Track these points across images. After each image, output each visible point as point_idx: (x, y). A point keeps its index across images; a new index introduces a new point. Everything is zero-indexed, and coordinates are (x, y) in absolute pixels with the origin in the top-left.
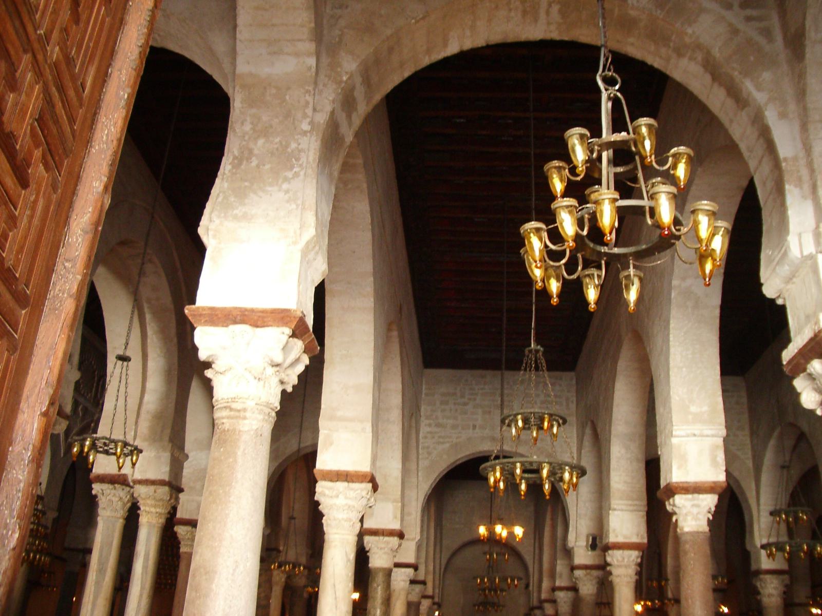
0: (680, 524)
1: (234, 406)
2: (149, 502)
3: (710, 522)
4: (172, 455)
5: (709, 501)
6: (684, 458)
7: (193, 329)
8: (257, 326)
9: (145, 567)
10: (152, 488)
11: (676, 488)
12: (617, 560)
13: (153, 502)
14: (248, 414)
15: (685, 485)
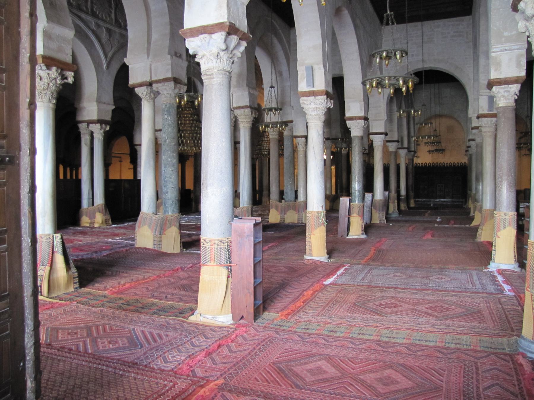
0: (498, 102)
1: (208, 73)
2: (242, 117)
3: (516, 101)
4: (249, 93)
5: (515, 88)
6: (499, 65)
7: (185, 40)
8: (212, 34)
9: (245, 148)
10: (243, 110)
11: (493, 82)
12: (485, 124)
13: (244, 117)
14: (214, 76)
15: (498, 80)
